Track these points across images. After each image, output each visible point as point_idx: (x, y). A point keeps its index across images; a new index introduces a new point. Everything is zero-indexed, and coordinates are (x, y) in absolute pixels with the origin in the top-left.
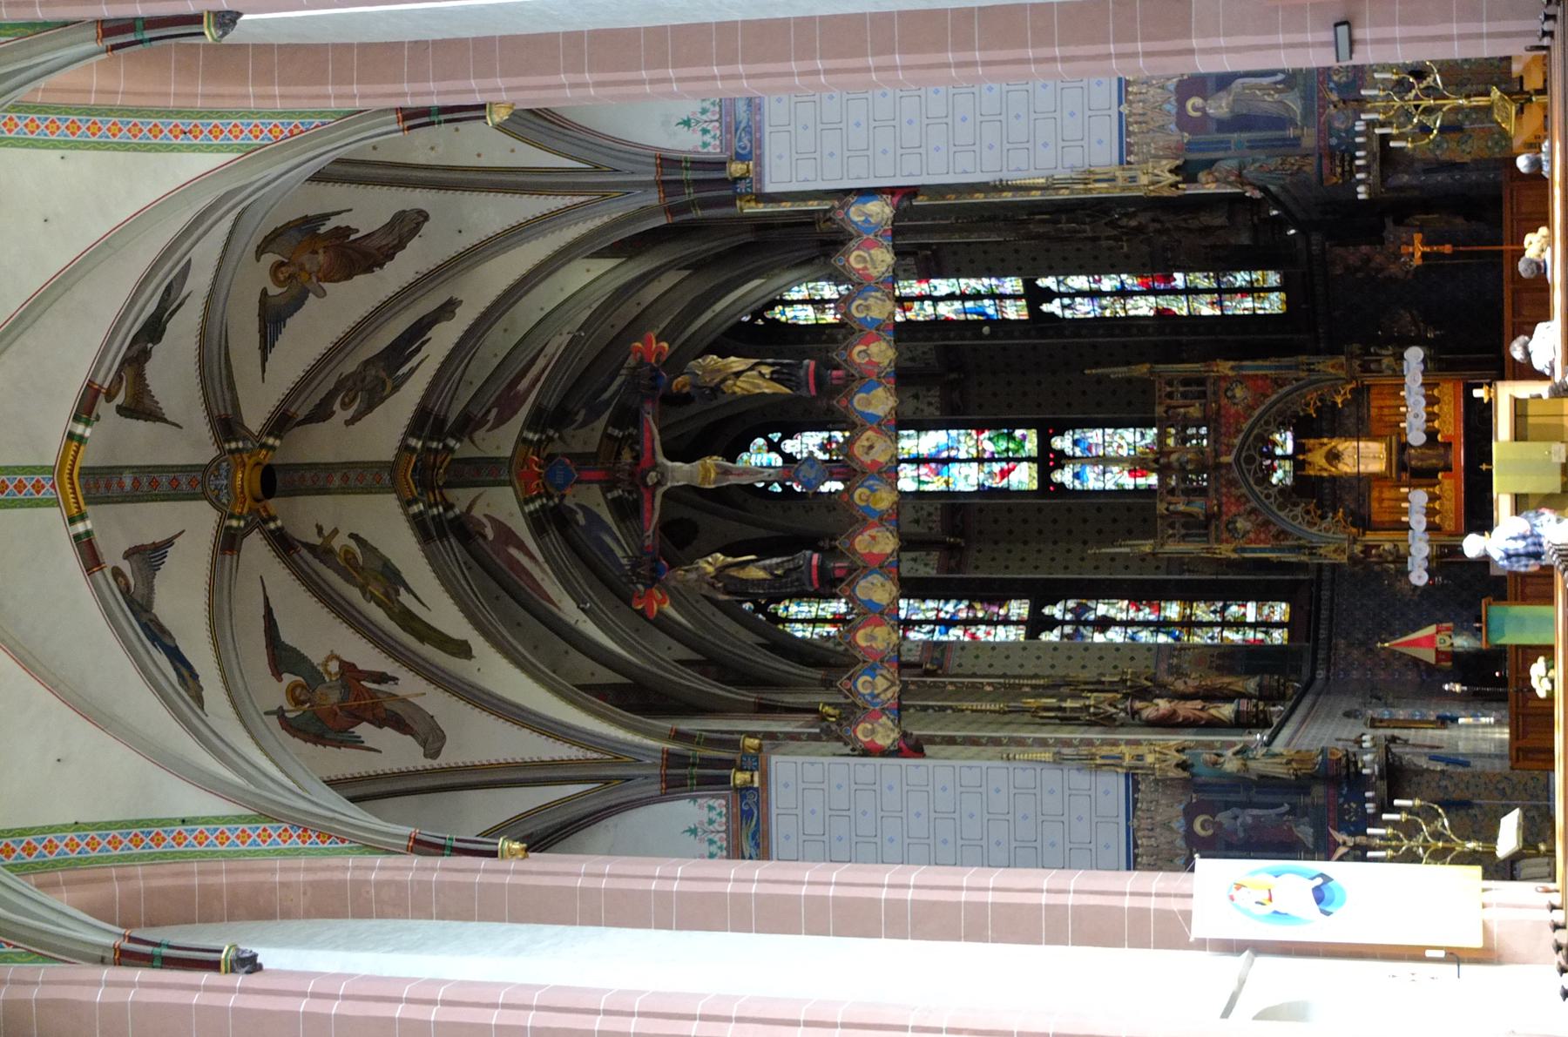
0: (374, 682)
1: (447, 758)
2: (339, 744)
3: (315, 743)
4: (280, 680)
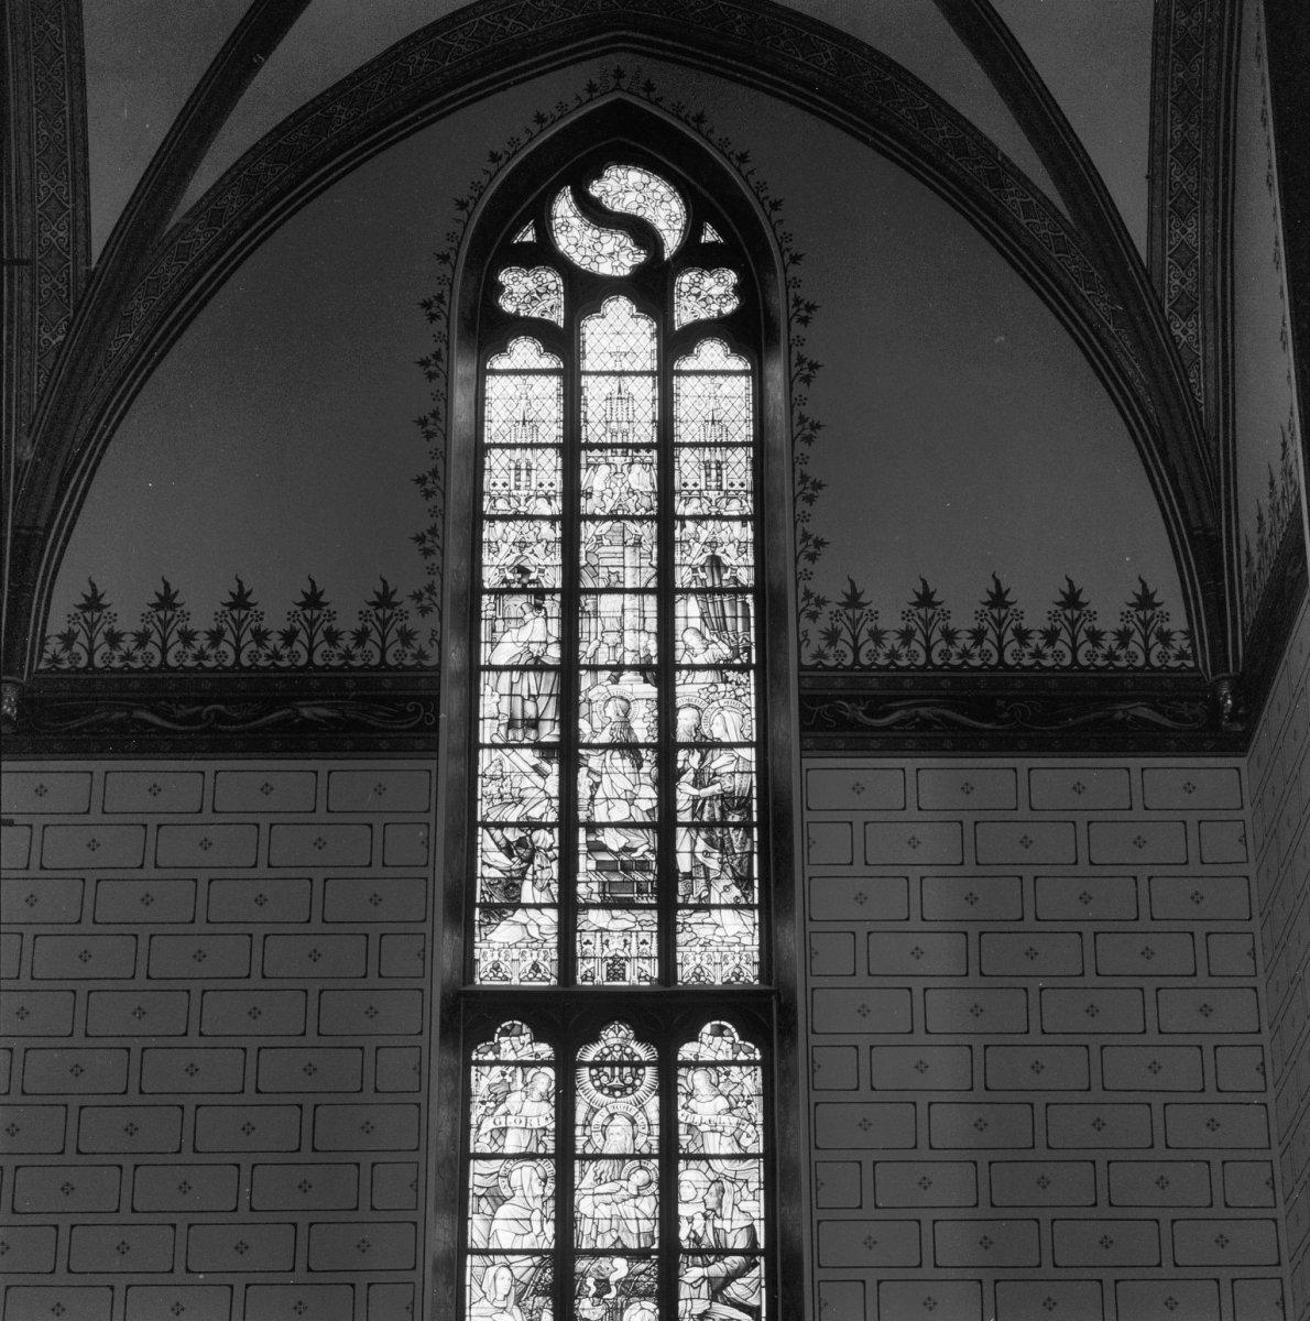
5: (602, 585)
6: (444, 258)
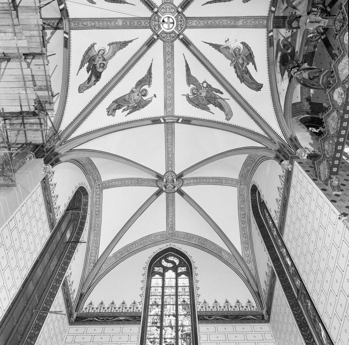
0: (216, 92)
1: (231, 122)
2: (203, 109)
3: (195, 107)
4: (190, 86)
5: (167, 304)
6: (147, 263)
